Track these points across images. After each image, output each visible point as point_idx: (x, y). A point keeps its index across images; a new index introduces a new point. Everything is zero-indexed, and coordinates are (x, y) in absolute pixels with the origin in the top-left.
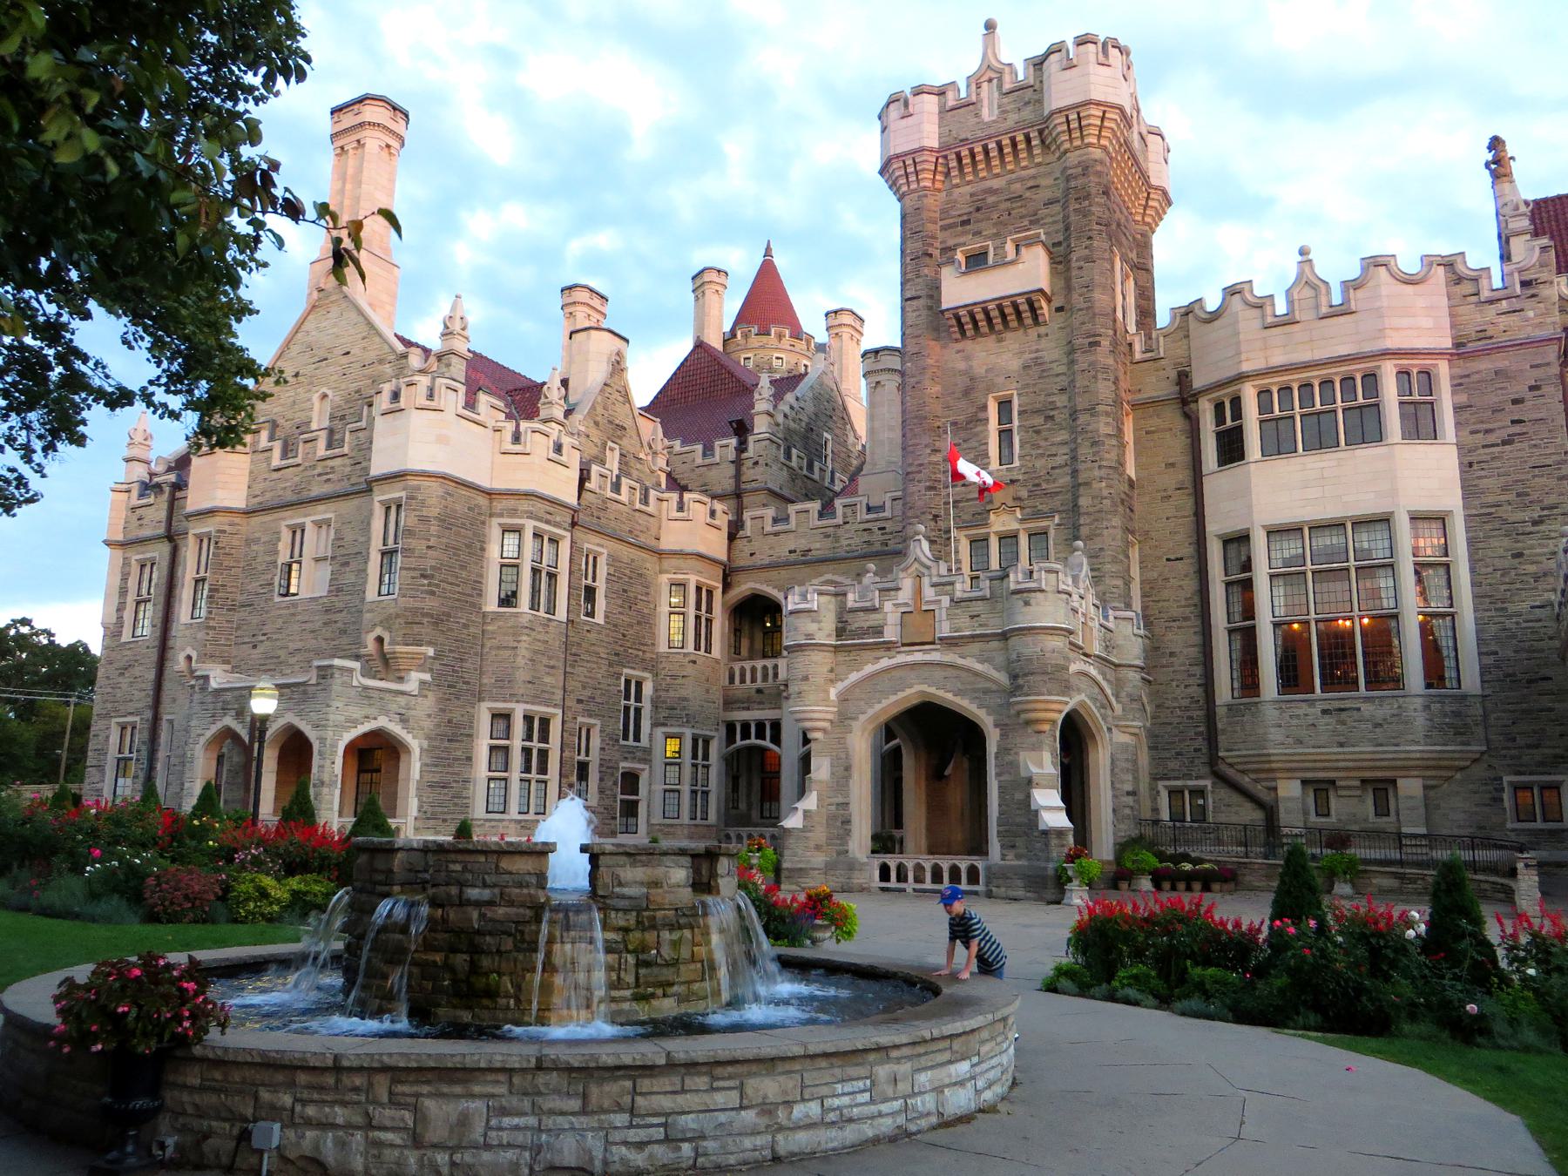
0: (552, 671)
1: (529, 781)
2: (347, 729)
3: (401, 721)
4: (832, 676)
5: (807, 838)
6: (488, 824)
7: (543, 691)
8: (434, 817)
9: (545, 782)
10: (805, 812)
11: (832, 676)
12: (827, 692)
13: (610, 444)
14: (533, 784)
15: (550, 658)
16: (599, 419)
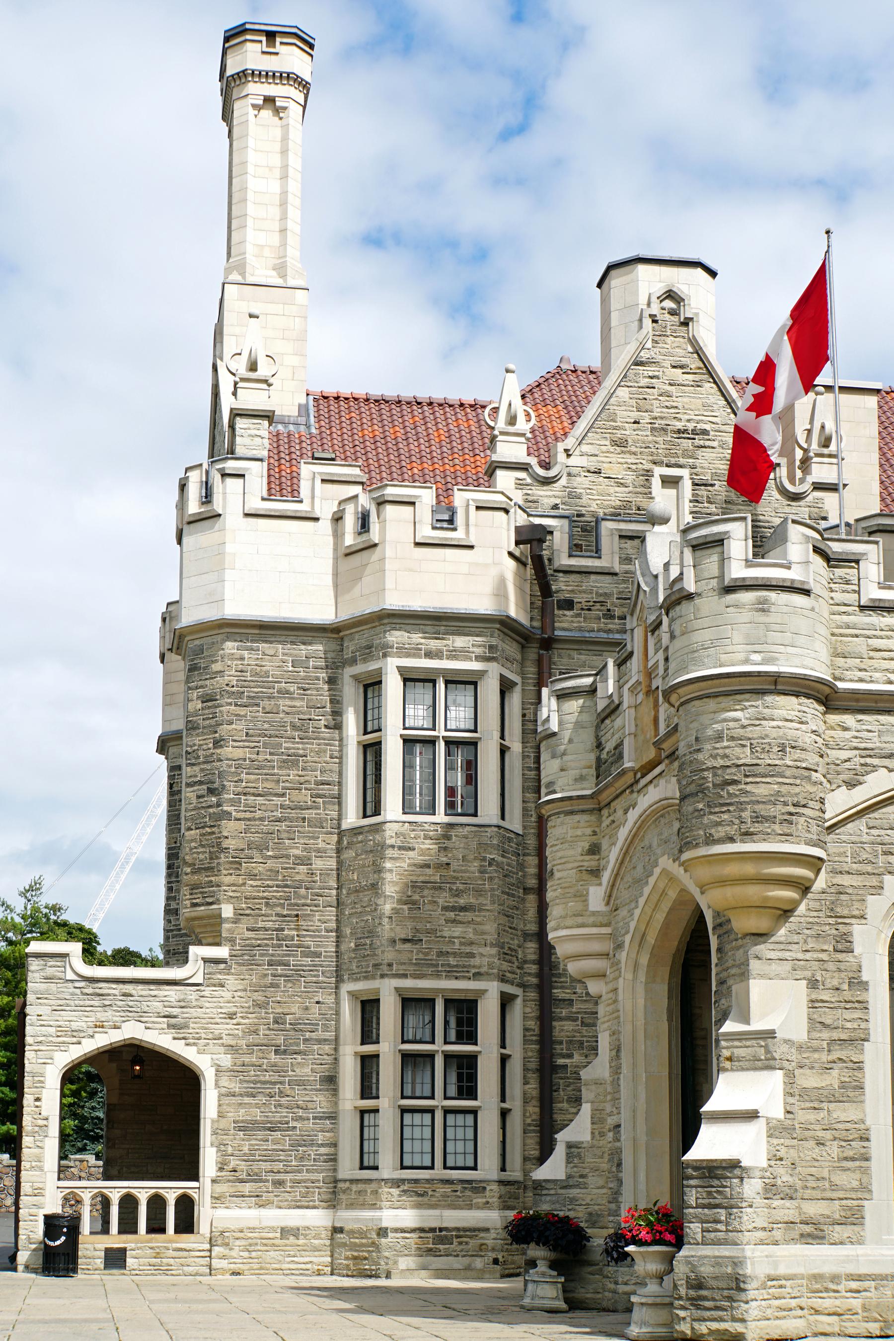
0: (468, 916)
1: (431, 1111)
2: (62, 1046)
3: (170, 1026)
4: (590, 862)
5: (573, 1200)
6: (354, 1188)
7: (441, 954)
8: (254, 1178)
9: (474, 1112)
10: (570, 1146)
11: (590, 862)
12: (583, 897)
13: (659, 471)
14: (439, 1115)
15: (458, 894)
16: (629, 431)
